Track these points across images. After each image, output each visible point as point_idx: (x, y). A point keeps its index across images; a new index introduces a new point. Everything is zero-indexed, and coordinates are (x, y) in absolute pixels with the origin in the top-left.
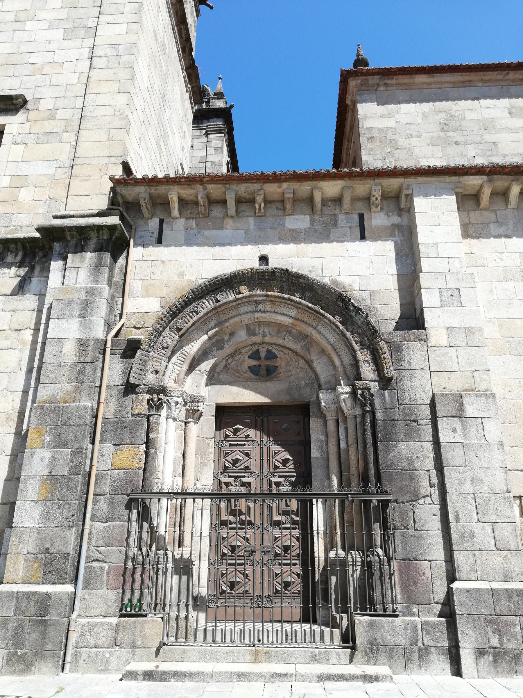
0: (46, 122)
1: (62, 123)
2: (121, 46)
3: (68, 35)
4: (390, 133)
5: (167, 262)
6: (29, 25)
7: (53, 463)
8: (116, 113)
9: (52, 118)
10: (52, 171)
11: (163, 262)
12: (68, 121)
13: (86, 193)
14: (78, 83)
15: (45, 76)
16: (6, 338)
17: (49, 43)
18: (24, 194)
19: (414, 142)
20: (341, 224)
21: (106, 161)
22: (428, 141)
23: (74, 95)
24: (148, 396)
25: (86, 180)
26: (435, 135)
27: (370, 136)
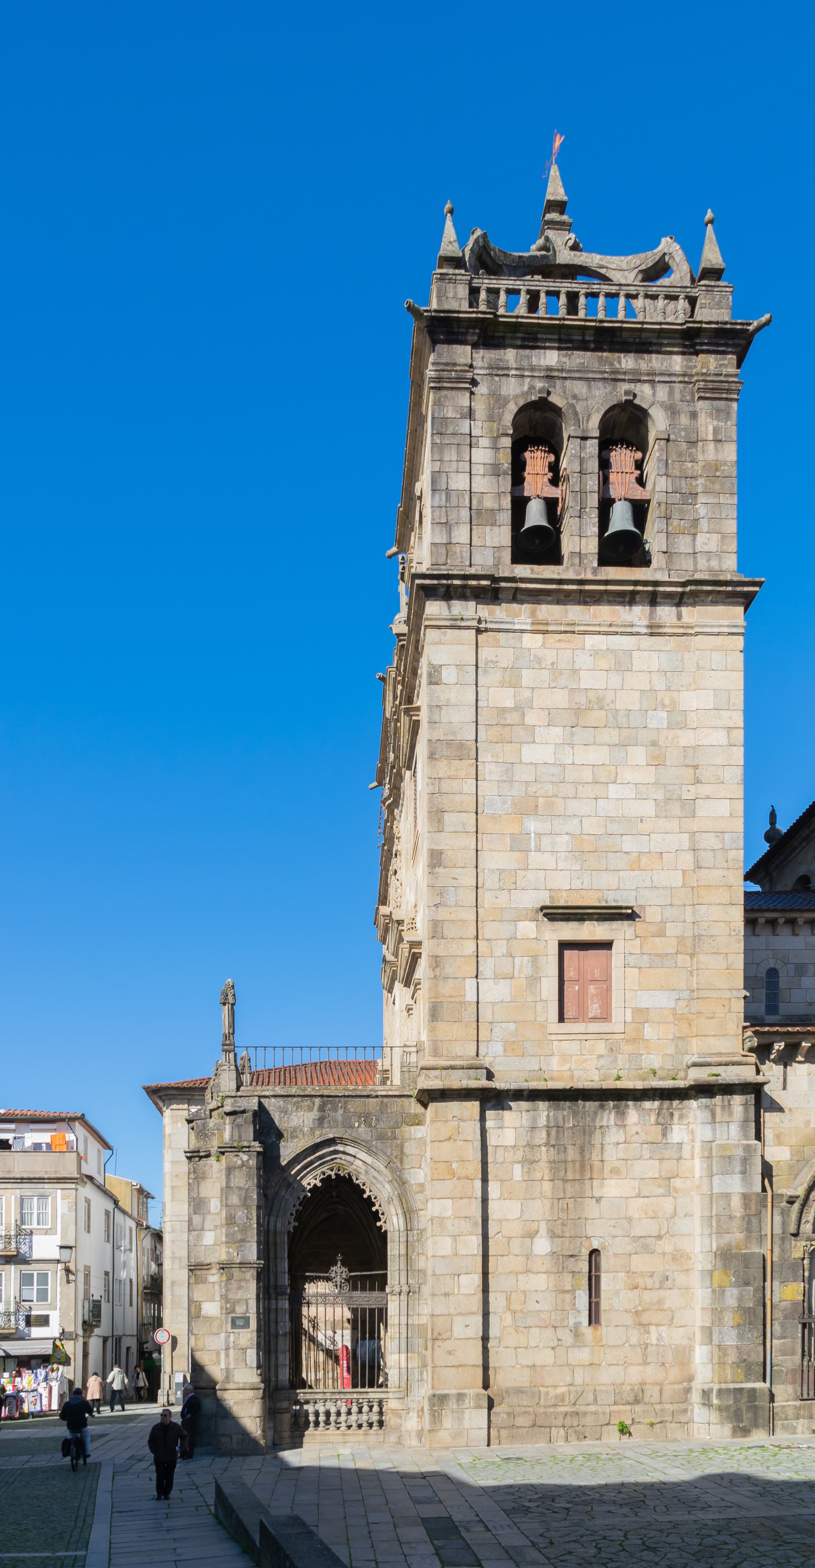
0: (657, 940)
1: (674, 942)
2: (726, 835)
3: (663, 807)
5: (794, 1110)
6: (613, 791)
8: (733, 933)
9: (662, 934)
12: (681, 939)
13: (713, 1033)
14: (684, 886)
15: (645, 873)
17: (641, 821)
18: (649, 1031)
21: (727, 995)
23: (681, 903)
25: (712, 1018)
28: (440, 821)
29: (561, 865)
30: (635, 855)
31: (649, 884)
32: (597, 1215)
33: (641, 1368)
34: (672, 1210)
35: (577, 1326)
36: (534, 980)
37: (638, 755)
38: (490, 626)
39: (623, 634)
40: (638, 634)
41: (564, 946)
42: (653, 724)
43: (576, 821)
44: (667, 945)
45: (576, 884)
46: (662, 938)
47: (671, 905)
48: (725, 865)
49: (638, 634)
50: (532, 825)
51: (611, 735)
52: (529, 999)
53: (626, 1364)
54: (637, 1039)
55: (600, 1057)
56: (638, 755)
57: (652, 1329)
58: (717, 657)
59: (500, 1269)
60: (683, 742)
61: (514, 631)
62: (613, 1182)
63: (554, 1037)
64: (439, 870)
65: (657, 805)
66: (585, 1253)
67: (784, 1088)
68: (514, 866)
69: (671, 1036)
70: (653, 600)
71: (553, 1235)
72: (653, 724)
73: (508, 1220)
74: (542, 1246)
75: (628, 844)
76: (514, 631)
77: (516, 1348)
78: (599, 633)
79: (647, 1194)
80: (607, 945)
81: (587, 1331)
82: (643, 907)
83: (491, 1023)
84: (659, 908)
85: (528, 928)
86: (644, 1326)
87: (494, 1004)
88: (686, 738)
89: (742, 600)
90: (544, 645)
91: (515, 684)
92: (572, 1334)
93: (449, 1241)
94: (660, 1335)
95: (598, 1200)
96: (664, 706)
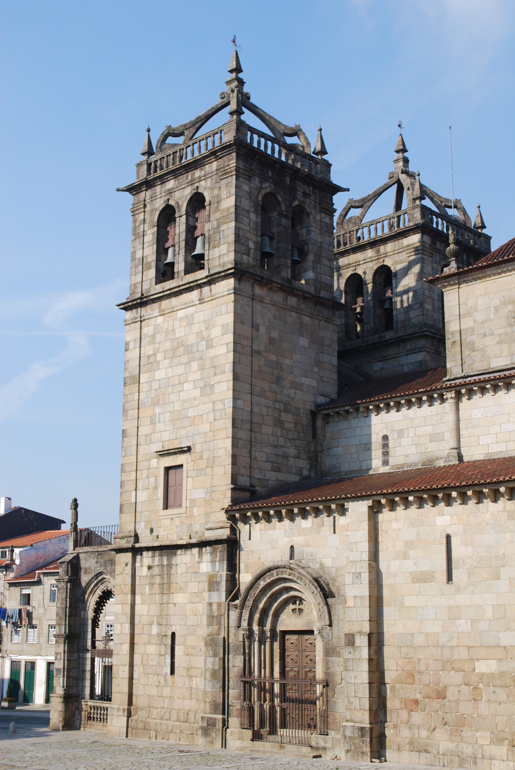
0: (199, 461)
1: (205, 461)
4: (469, 334)
6: (186, 386)
7: (213, 664)
9: (201, 458)
10: (204, 496)
11: (252, 552)
14: (210, 431)
16: (198, 597)
18: (196, 511)
19: (488, 341)
20: (325, 524)
21: (224, 488)
22: (498, 339)
24: (243, 632)
26: (503, 331)
27: (453, 340)
28: (127, 415)
29: (167, 428)
30: (192, 418)
31: (197, 432)
32: (174, 614)
33: (189, 701)
34: (202, 611)
35: (166, 673)
36: (156, 488)
37: (195, 365)
38: (146, 318)
39: (190, 307)
40: (195, 305)
41: (167, 469)
42: (200, 349)
43: (172, 404)
44: (202, 464)
45: (172, 438)
46: (202, 460)
47: (205, 442)
48: (225, 417)
49: (195, 305)
50: (157, 410)
51: (185, 359)
52: (154, 499)
53: (184, 698)
54: (191, 516)
55: (177, 527)
56: (195, 365)
57: (194, 678)
58: (224, 308)
59: (140, 642)
60: (212, 355)
61: (153, 317)
62: (181, 594)
63: (161, 518)
64: (125, 439)
65: (201, 390)
66: (170, 634)
67: (250, 539)
68: (150, 432)
69: (203, 513)
70: (200, 286)
71: (159, 624)
72: (200, 349)
73: (143, 615)
74: (155, 630)
75: (191, 413)
76: (153, 317)
77: (144, 685)
78: (182, 309)
79: (192, 601)
80: (181, 466)
81: (169, 677)
82: (194, 445)
83: (141, 512)
84: (200, 445)
85: (154, 462)
86: (191, 677)
87: (142, 502)
88: (212, 353)
89: (232, 276)
90: (164, 321)
91: (153, 342)
92: (164, 679)
93: (119, 625)
94: (197, 683)
95: (175, 604)
96: (204, 338)
